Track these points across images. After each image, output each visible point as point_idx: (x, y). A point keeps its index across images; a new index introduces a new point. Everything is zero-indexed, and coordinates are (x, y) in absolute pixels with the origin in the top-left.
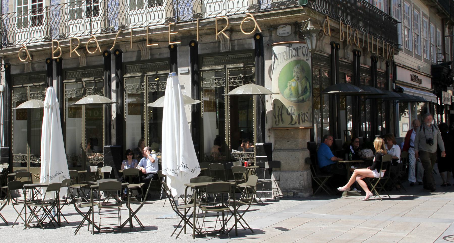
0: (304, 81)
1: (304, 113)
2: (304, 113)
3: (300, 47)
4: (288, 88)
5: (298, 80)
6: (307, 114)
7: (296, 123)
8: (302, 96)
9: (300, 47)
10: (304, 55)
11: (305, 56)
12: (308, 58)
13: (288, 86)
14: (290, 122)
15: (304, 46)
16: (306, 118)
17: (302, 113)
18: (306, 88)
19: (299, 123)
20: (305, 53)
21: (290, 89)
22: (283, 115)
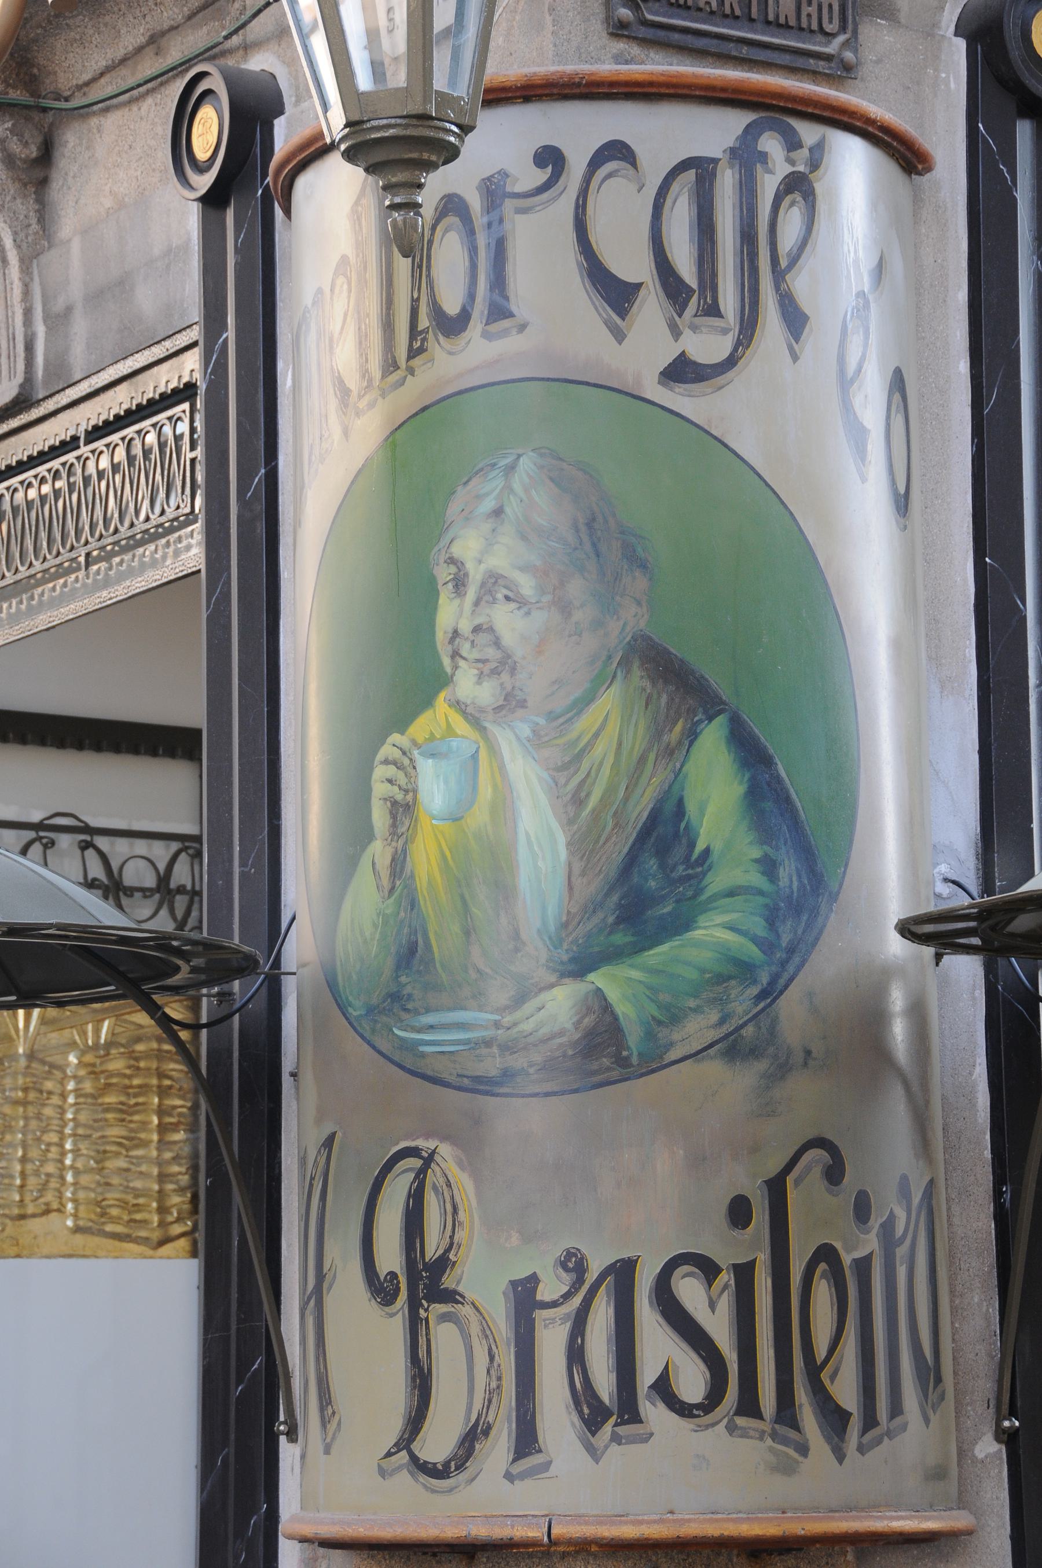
0: (613, 719)
1: (623, 1273)
2: (623, 1273)
3: (550, 158)
4: (379, 851)
5: (511, 703)
6: (690, 1290)
7: (473, 1436)
8: (580, 967)
9: (550, 158)
10: (616, 294)
11: (651, 307)
12: (708, 346)
13: (379, 817)
14: (394, 1426)
15: (616, 152)
16: (658, 1346)
17: (574, 1264)
18: (664, 832)
19: (526, 1441)
20: (632, 263)
21: (399, 864)
22: (329, 1300)
